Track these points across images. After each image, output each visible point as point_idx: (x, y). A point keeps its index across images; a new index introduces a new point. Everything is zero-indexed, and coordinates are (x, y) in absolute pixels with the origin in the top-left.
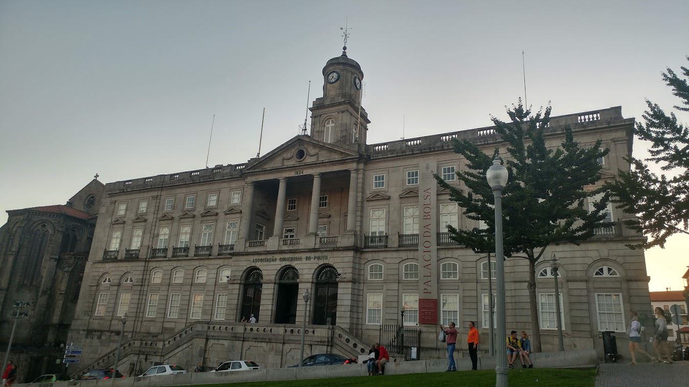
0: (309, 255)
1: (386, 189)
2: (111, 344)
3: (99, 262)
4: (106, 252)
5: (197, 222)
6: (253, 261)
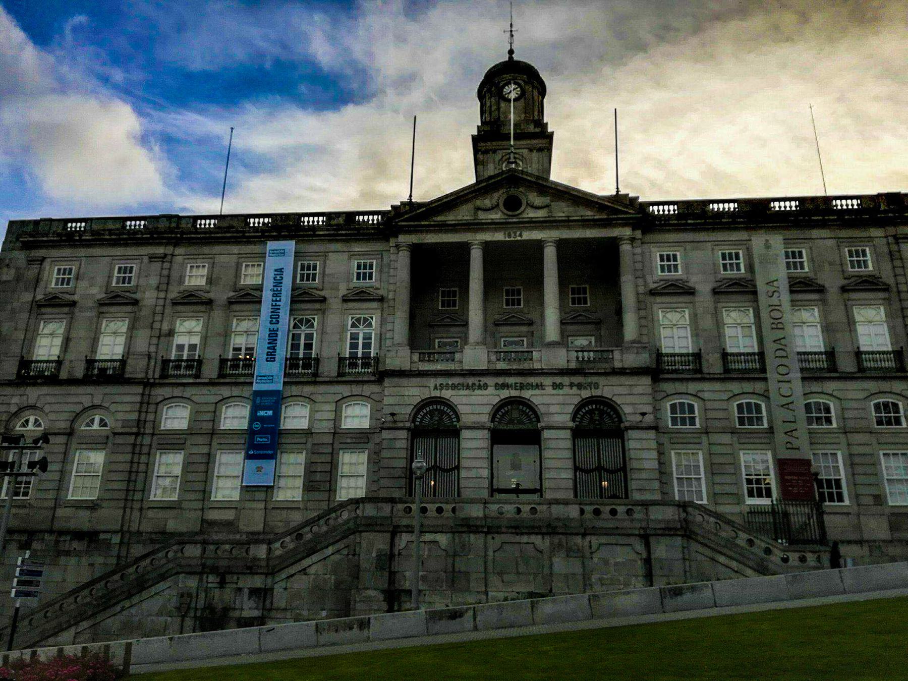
0: (558, 380)
1: (684, 277)
2: (63, 560)
3: (10, 383)
6: (436, 388)
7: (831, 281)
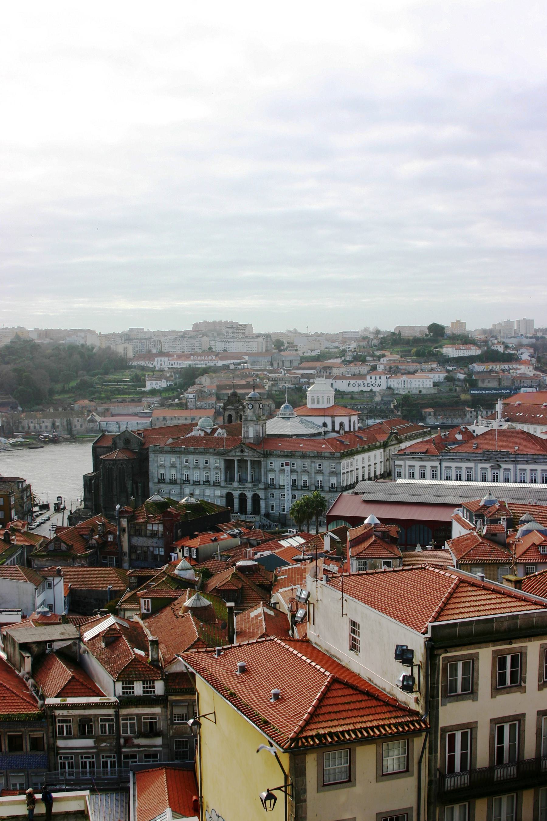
4: (159, 479)
5: (202, 470)
7: (299, 470)
